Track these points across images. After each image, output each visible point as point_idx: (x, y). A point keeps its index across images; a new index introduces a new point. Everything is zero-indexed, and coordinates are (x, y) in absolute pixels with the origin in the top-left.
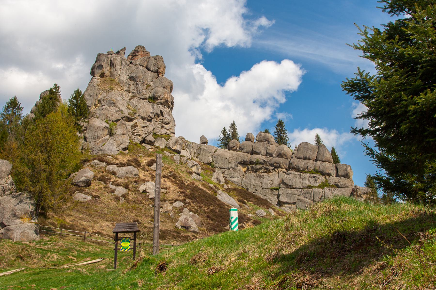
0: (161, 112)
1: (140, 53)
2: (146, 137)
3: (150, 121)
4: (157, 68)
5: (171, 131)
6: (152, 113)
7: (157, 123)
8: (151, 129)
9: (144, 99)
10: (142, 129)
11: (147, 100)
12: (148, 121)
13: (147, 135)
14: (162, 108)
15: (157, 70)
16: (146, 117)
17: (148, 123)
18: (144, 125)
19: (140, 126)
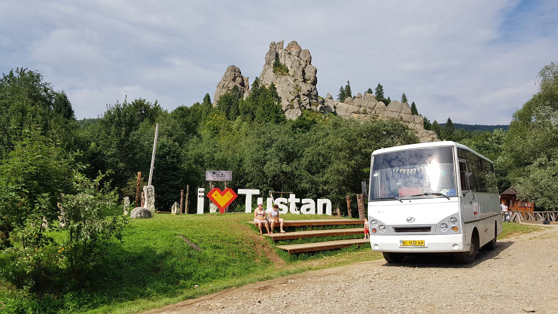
1: (294, 46)
3: (306, 96)
8: (308, 101)
17: (306, 98)
19: (303, 99)
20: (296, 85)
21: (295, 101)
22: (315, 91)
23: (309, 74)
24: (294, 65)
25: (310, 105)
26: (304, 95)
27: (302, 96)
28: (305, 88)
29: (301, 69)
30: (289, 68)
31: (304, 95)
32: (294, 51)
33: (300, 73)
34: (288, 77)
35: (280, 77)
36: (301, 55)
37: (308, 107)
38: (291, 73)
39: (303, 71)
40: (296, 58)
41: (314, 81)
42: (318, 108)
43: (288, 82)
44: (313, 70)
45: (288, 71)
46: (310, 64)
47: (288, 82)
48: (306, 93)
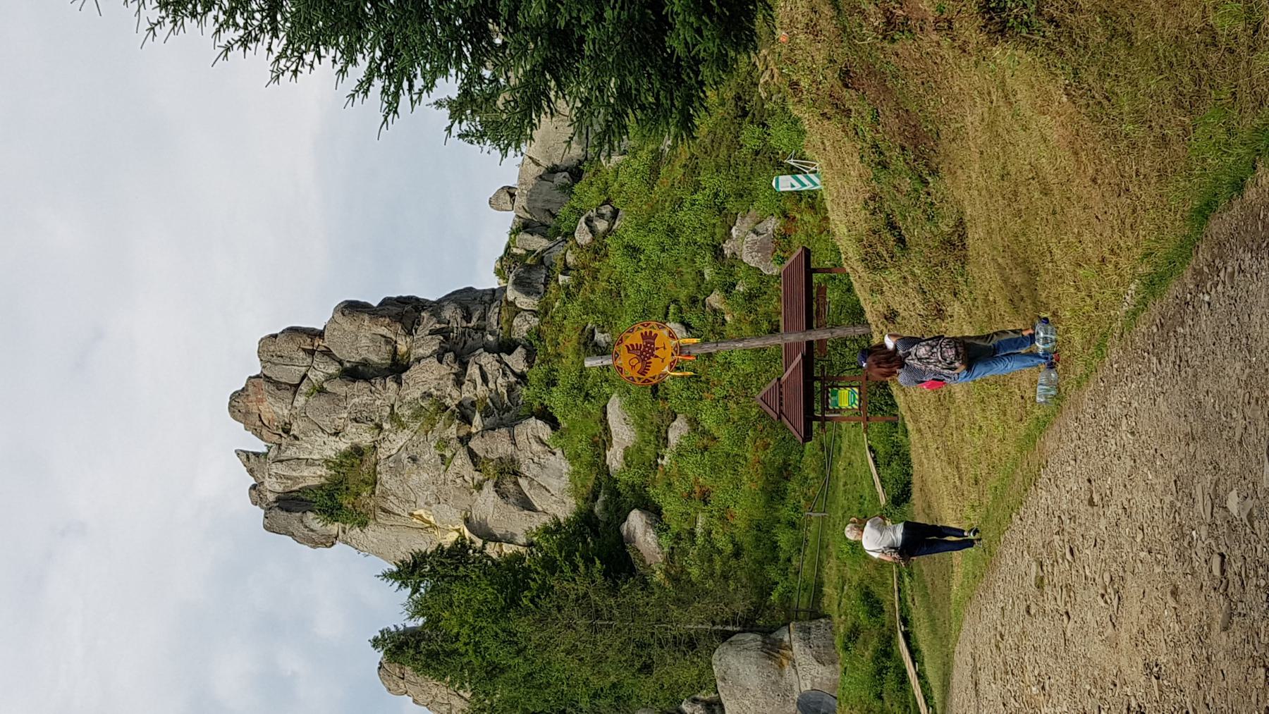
0: (432, 333)
2: (513, 372)
3: (464, 366)
4: (301, 354)
5: (487, 298)
6: (440, 361)
7: (470, 342)
9: (400, 384)
10: (491, 385)
11: (404, 376)
12: (466, 370)
13: (509, 372)
14: (422, 331)
15: (304, 350)
16: (452, 376)
17: (473, 371)
18: (479, 381)
19: (481, 390)
20: (415, 417)
21: (475, 444)
22: (447, 313)
23: (365, 343)
24: (325, 422)
25: (507, 346)
26: (459, 383)
27: (467, 393)
28: (429, 376)
29: (339, 388)
30: (343, 445)
31: (459, 383)
32: (274, 408)
33: (359, 395)
34: (382, 453)
35: (384, 496)
36: (289, 374)
37: (517, 361)
38: (366, 439)
39: (355, 373)
40: (300, 400)
41: (399, 318)
42: (524, 301)
43: (404, 456)
44: (347, 324)
45: (357, 451)
46: (320, 334)
47: (404, 456)
48: (446, 370)
